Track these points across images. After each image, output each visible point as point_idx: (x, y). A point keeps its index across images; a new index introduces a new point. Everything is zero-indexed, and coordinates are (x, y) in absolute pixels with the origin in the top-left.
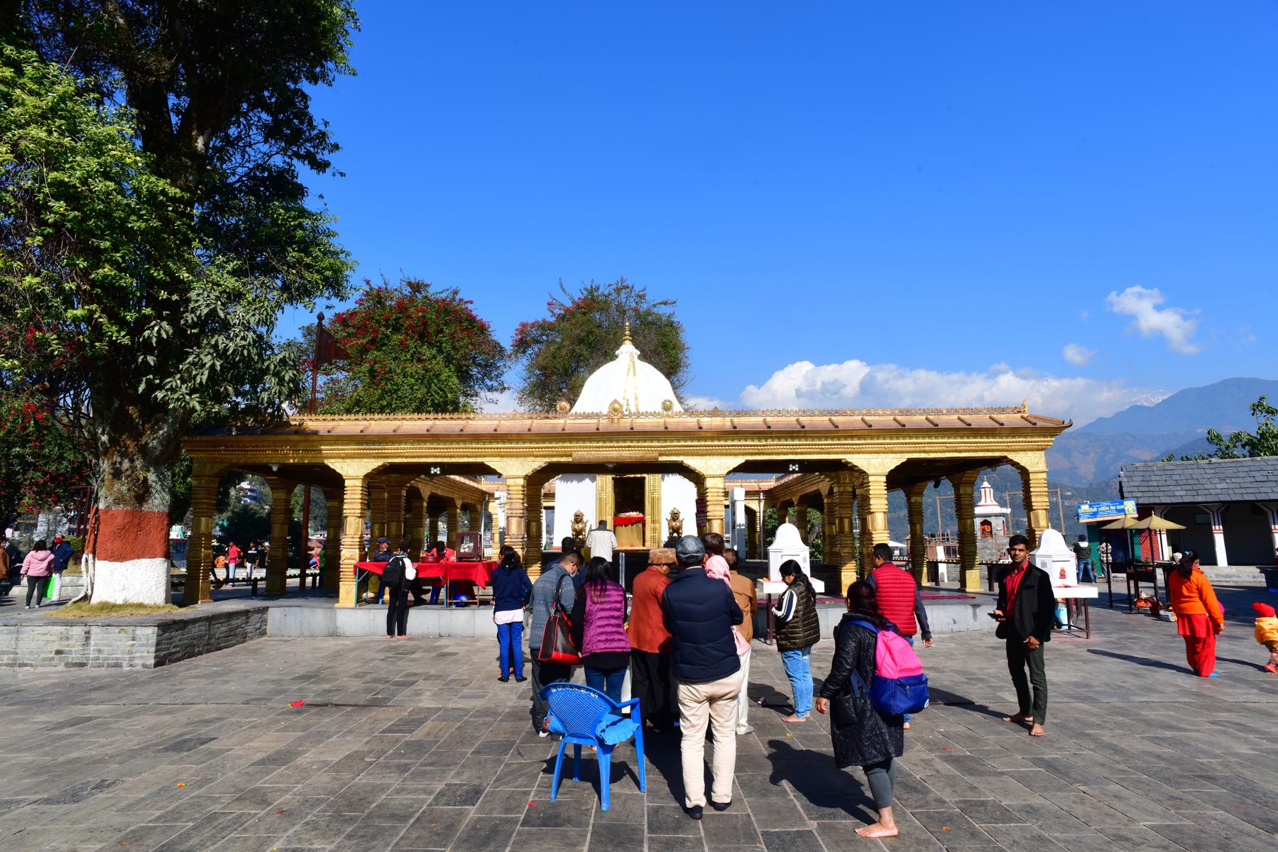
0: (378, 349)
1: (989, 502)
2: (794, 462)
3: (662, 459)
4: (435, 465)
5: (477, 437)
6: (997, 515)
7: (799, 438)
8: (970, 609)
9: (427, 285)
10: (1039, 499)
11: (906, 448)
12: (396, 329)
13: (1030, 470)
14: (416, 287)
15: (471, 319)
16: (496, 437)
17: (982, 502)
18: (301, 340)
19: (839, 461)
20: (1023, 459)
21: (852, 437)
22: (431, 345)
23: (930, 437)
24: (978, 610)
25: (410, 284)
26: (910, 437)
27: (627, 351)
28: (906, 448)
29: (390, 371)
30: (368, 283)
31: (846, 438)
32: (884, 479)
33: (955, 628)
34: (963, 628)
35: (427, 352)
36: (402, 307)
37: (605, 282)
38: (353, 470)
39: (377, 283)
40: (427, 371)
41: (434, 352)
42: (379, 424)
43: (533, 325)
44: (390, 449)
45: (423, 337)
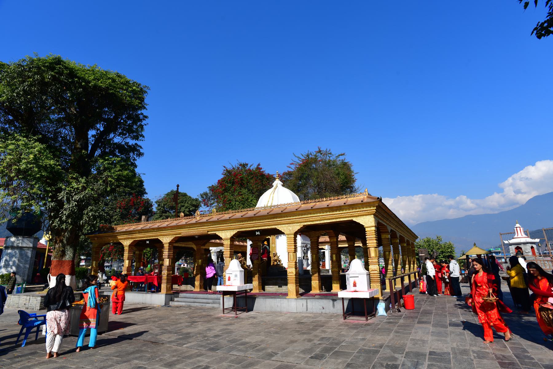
0: (227, 192)
1: (520, 235)
2: (258, 230)
3: (209, 233)
4: (147, 240)
5: (153, 230)
6: (525, 243)
7: (255, 220)
8: (331, 302)
9: (247, 165)
10: (371, 242)
11: (301, 220)
12: (233, 184)
13: (365, 226)
14: (244, 165)
15: (262, 175)
16: (159, 229)
17: (516, 236)
18: (208, 192)
19: (276, 229)
20: (360, 220)
21: (276, 218)
22: (245, 188)
23: (311, 214)
24: (335, 302)
25: (241, 165)
26: (302, 215)
27: (277, 183)
28: (301, 220)
29: (230, 200)
30: (225, 167)
31: (274, 218)
32: (293, 236)
33: (324, 311)
34: (327, 311)
35: (244, 191)
36: (235, 175)
37: (313, 150)
38: (126, 243)
39: (229, 167)
40: (243, 198)
41: (246, 190)
42: (133, 227)
43: (284, 174)
44: (134, 236)
45: (242, 185)
